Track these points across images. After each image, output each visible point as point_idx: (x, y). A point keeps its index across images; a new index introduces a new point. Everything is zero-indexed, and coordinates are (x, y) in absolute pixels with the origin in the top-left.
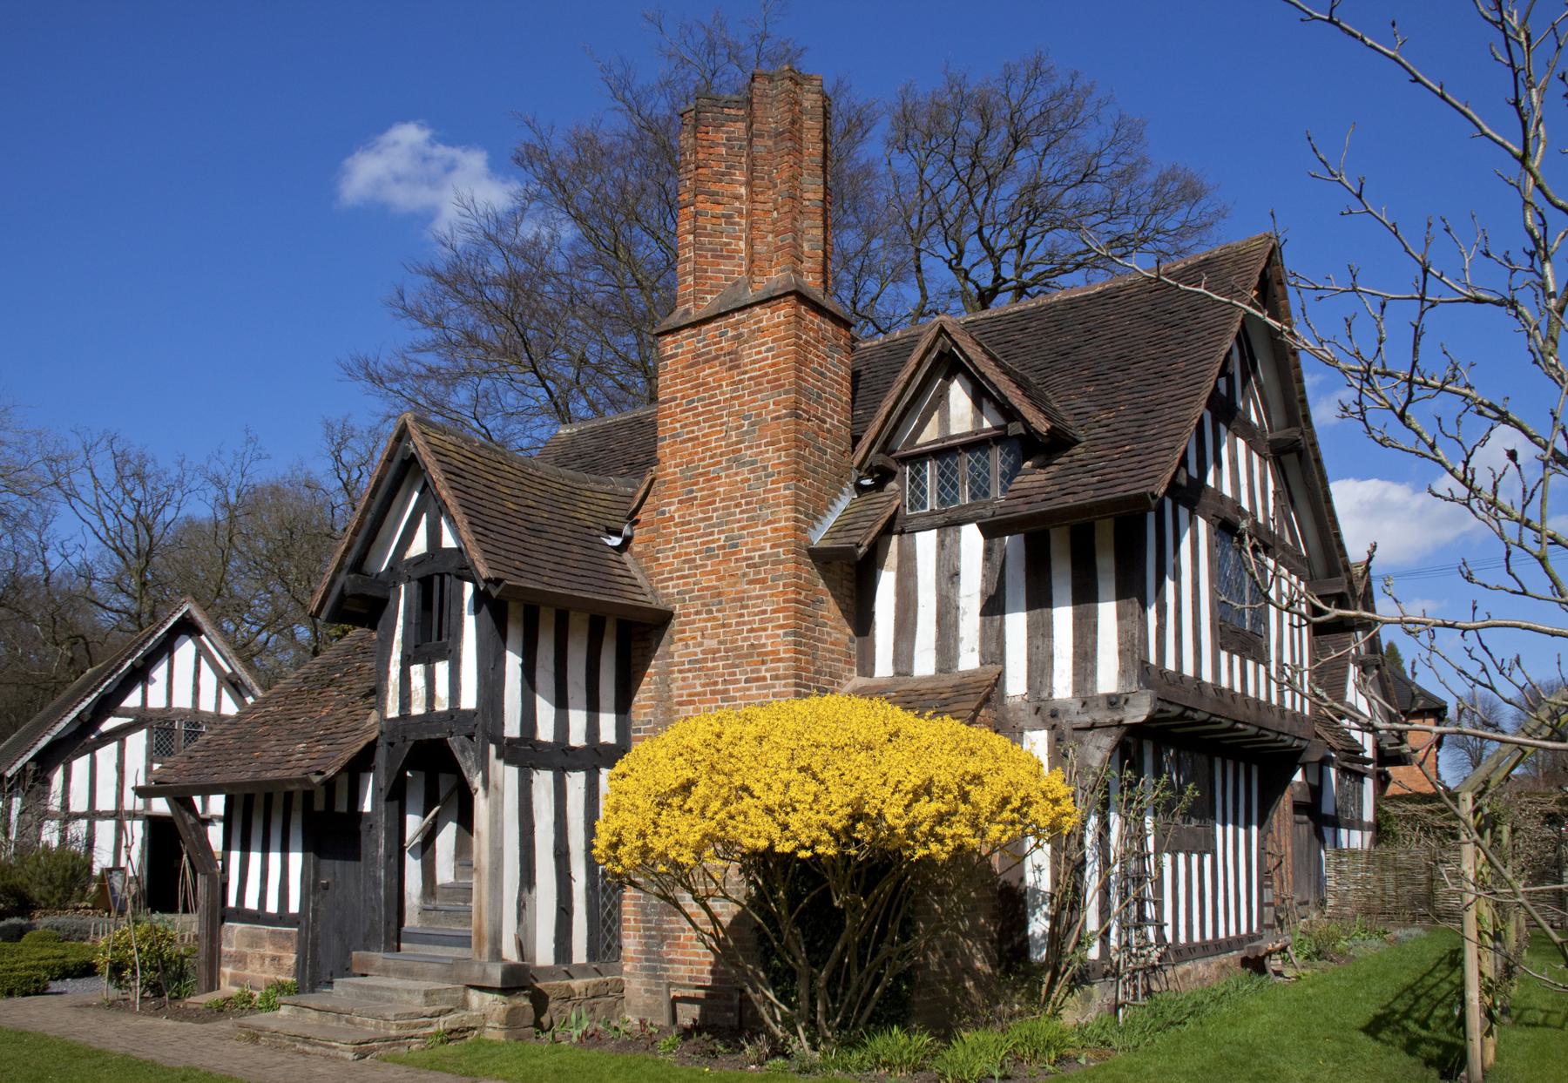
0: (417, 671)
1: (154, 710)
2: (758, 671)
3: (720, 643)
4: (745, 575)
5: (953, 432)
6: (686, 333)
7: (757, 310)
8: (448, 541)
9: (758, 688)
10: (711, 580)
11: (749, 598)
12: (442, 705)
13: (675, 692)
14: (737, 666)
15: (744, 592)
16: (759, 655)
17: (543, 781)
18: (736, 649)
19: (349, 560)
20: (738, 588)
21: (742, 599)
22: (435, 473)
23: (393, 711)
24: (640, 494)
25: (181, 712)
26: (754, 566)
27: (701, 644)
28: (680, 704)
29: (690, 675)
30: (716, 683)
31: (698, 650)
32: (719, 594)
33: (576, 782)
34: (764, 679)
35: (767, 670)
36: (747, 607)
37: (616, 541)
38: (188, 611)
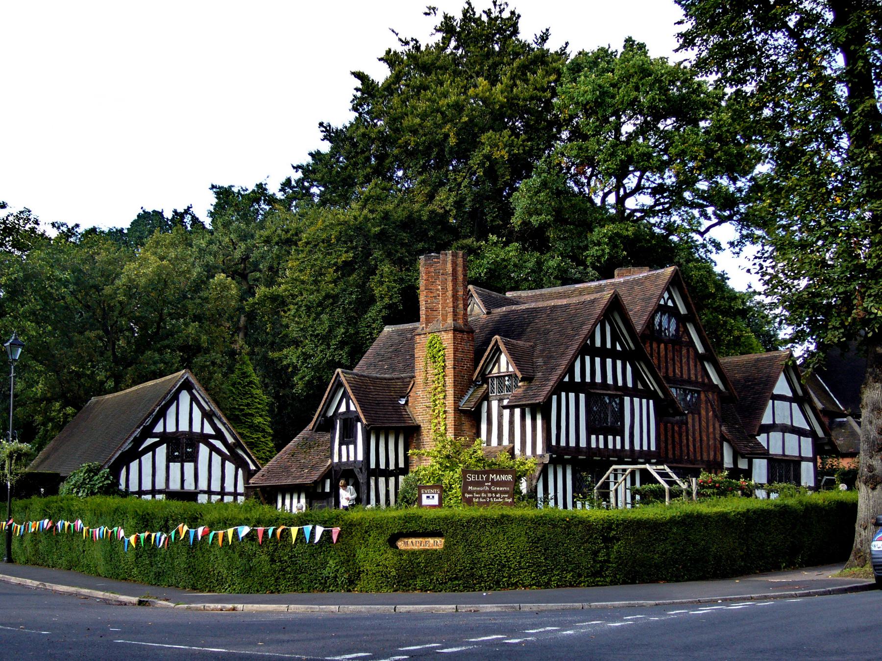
0: (344, 448)
1: (169, 433)
5: (502, 371)
6: (423, 336)
7: (443, 333)
8: (352, 408)
12: (352, 458)
17: (382, 480)
19: (322, 413)
22: (347, 385)
23: (336, 460)
24: (410, 387)
25: (183, 433)
33: (392, 480)
37: (403, 402)
38: (187, 378)
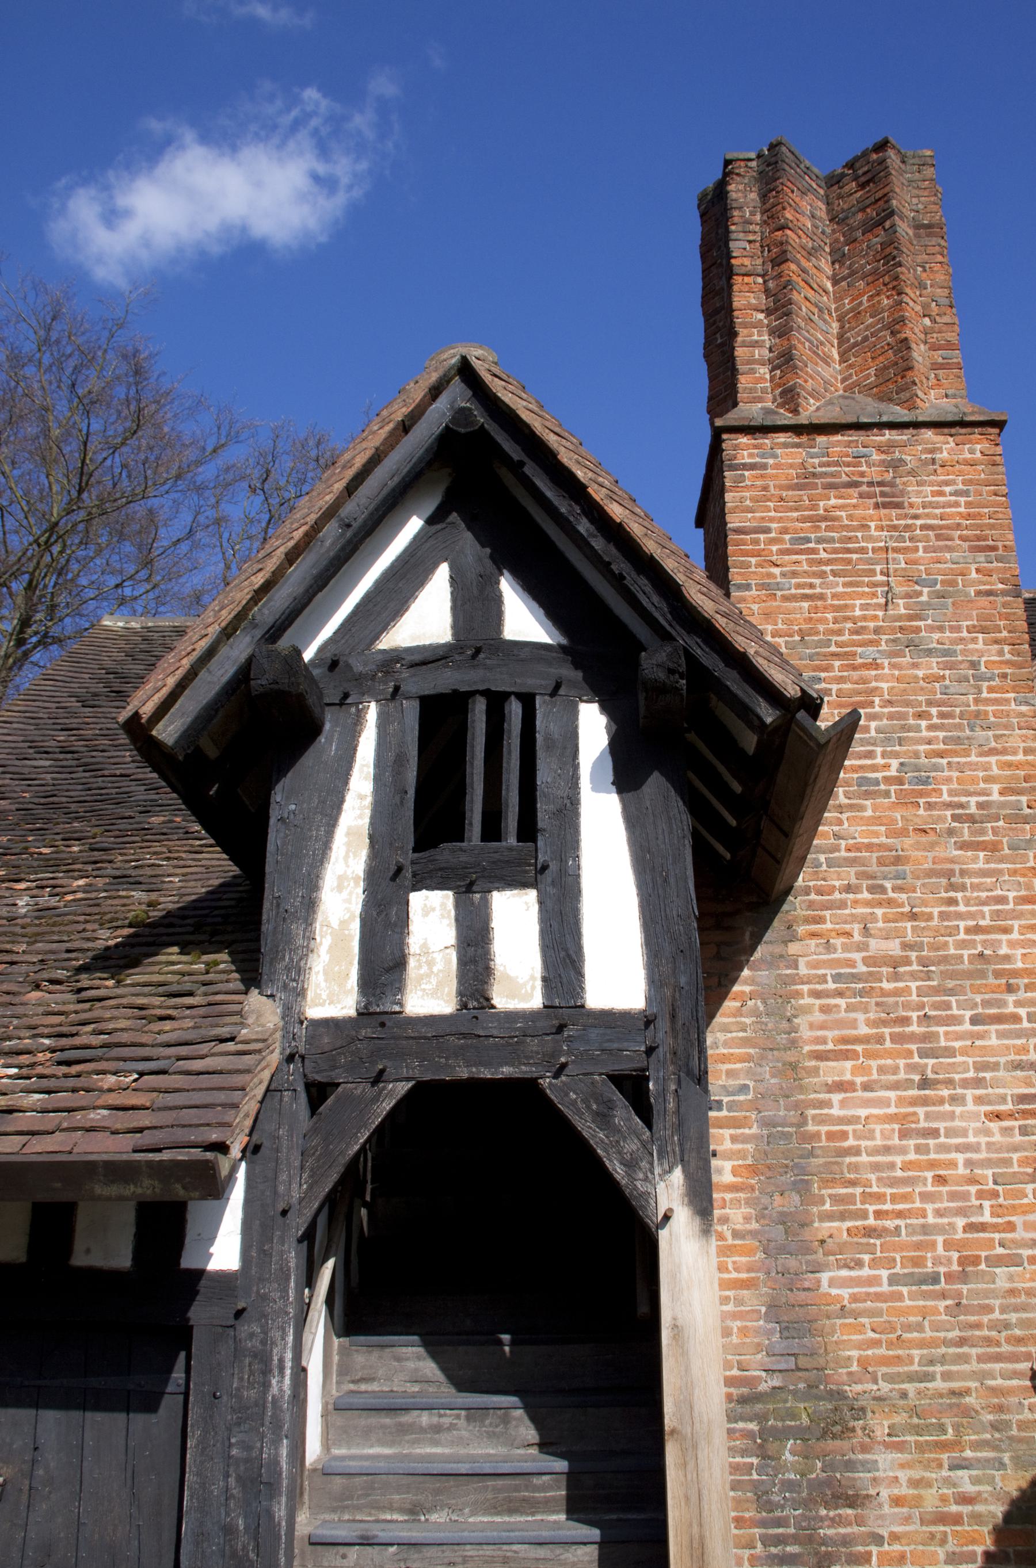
2: (1002, 1003)
3: (905, 946)
4: (951, 832)
9: (1001, 1035)
10: (877, 834)
11: (963, 873)
13: (806, 1033)
14: (951, 992)
15: (952, 861)
16: (998, 974)
18: (945, 960)
20: (940, 852)
21: (950, 874)
26: (971, 819)
27: (862, 947)
28: (820, 1056)
29: (842, 1002)
30: (905, 1021)
31: (857, 956)
32: (898, 860)
34: (1016, 1018)
35: (1018, 1004)
36: (963, 888)
